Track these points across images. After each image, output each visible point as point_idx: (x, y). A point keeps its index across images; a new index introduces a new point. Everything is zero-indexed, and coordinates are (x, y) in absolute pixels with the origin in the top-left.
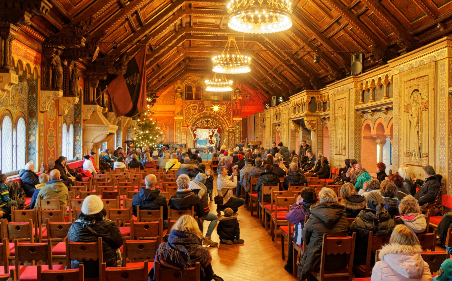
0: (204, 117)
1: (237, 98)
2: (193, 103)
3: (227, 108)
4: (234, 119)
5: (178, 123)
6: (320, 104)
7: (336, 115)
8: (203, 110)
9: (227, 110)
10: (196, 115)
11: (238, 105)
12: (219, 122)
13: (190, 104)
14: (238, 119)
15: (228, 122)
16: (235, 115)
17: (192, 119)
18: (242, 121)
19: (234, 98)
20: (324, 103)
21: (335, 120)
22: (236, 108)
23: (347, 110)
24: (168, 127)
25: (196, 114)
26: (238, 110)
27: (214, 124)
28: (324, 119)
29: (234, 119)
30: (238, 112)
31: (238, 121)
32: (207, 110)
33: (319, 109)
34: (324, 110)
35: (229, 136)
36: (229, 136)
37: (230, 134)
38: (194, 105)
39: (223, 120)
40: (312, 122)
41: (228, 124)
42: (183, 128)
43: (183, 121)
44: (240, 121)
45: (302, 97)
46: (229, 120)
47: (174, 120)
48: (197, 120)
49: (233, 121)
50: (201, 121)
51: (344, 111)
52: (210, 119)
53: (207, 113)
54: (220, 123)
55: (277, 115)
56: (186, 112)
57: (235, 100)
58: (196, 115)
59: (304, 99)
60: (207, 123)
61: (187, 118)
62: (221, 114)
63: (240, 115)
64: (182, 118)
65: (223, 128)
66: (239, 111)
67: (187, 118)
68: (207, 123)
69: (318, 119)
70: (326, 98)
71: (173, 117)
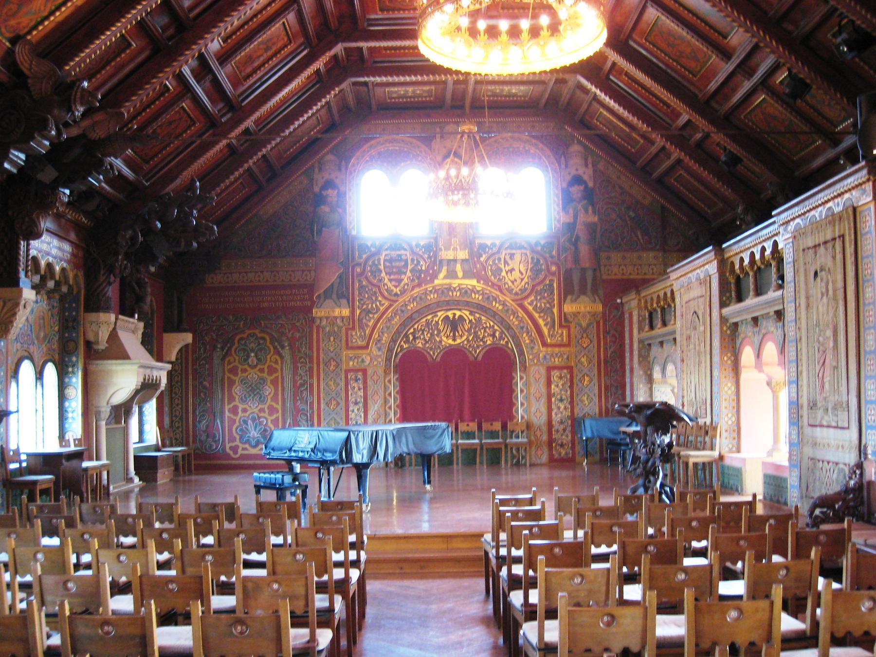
1: (576, 217)
4: (568, 308)
5: (330, 334)
8: (435, 276)
10: (406, 298)
12: (502, 322)
14: (583, 307)
15: (541, 322)
16: (568, 290)
18: (604, 314)
24: (286, 353)
25: (403, 292)
26: (583, 271)
27: (481, 334)
29: (568, 308)
30: (583, 280)
31: (584, 316)
32: (452, 274)
35: (549, 383)
36: (549, 383)
37: (555, 374)
39: (521, 313)
41: (545, 330)
42: (351, 353)
43: (352, 323)
44: (594, 315)
46: (546, 312)
47: (313, 319)
48: (411, 318)
49: (565, 321)
50: (428, 323)
52: (466, 314)
53: (449, 288)
54: (509, 328)
56: (361, 287)
58: (406, 298)
60: (454, 329)
61: (369, 312)
62: (510, 290)
63: (595, 291)
64: (346, 312)
65: (521, 353)
67: (369, 312)
68: (454, 329)
71: (309, 310)
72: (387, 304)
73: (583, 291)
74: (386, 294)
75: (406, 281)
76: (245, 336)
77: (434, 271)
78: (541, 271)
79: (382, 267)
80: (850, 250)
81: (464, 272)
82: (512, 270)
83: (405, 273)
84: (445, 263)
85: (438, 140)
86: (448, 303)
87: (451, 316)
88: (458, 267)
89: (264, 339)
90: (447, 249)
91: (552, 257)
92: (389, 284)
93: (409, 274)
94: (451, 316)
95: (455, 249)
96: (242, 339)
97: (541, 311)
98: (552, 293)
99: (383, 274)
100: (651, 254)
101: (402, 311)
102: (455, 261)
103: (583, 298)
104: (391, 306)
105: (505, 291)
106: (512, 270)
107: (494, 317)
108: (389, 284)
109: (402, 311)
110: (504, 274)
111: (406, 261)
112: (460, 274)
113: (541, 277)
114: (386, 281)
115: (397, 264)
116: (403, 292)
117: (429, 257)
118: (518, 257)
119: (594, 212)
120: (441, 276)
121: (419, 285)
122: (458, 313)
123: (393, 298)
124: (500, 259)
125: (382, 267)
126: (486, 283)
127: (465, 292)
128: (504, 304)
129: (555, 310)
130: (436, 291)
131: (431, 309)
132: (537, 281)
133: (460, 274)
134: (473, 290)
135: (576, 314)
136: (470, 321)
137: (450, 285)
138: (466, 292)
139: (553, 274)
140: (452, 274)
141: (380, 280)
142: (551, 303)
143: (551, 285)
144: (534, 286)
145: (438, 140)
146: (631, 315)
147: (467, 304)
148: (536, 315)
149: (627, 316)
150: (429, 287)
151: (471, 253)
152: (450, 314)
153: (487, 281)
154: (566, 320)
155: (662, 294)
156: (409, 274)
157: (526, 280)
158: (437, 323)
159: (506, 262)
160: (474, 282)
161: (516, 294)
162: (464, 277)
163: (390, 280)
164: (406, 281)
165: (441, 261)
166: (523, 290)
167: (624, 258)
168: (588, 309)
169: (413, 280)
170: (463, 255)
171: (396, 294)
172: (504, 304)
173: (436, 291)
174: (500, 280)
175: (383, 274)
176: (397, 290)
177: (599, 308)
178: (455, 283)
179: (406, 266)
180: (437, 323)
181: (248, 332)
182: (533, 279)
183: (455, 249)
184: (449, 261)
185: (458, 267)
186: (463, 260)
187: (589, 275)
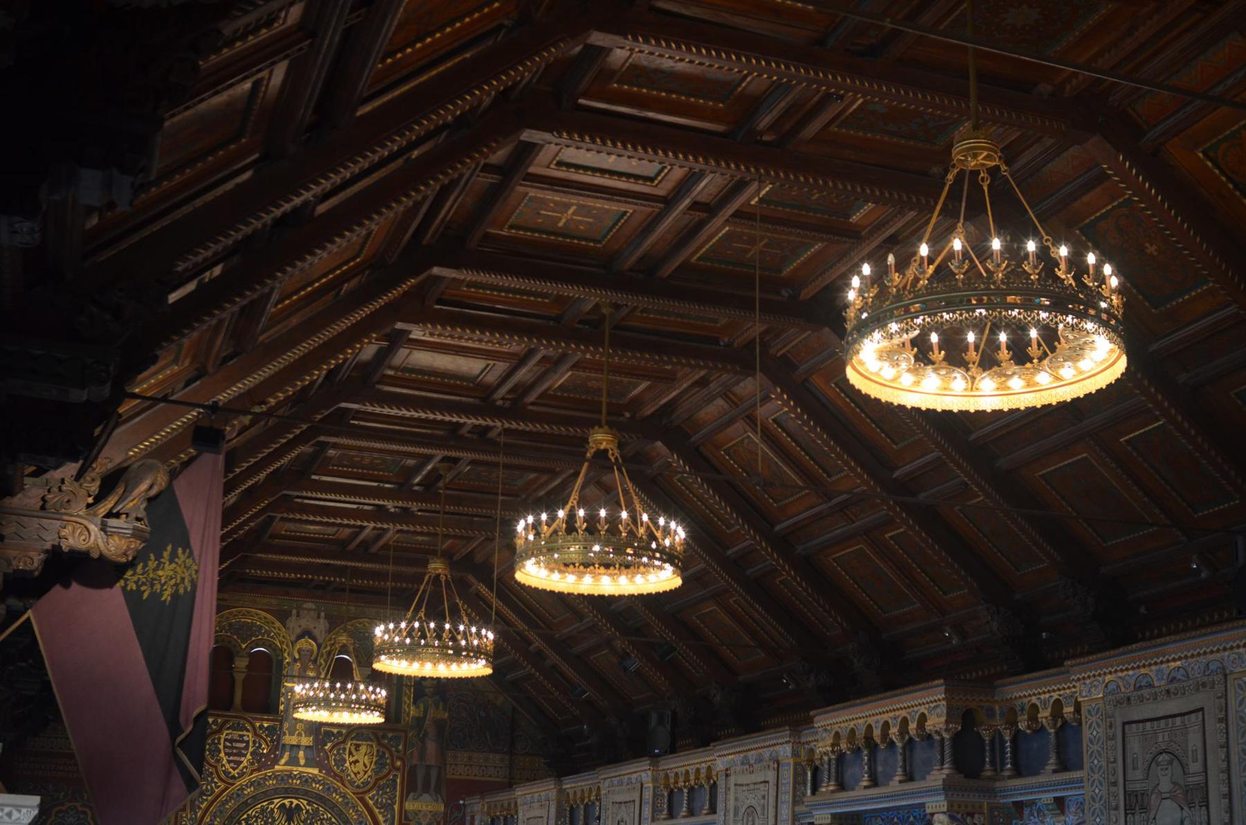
0: (276, 792)
1: (426, 712)
2: (232, 728)
3: (381, 756)
4: (409, 806)
6: (997, 738)
7: (1138, 787)
9: (380, 764)
10: (244, 781)
11: (431, 746)
13: (219, 731)
16: (411, 788)
17: (223, 797)
18: (445, 813)
19: (413, 711)
20: (1017, 736)
21: (1129, 809)
22: (422, 757)
23: (1216, 761)
25: (242, 774)
26: (429, 767)
28: (1019, 806)
29: (409, 806)
31: (425, 815)
33: (993, 763)
34: (1018, 772)
38: (236, 734)
39: (361, 808)
40: (969, 820)
44: (435, 814)
45: (928, 707)
46: (387, 808)
48: (246, 804)
50: (263, 810)
51: (1195, 767)
53: (290, 776)
55: (671, 793)
57: (419, 721)
58: (244, 781)
59: (923, 719)
62: (352, 782)
66: (434, 773)
69: (992, 808)
70: (1044, 714)
72: (223, 786)
73: (426, 789)
74: (223, 776)
75: (245, 763)
76: (64, 808)
77: (276, 756)
78: (383, 766)
79: (221, 747)
80: (637, 812)
81: (307, 759)
82: (356, 762)
83: (245, 756)
84: (288, 748)
85: (294, 618)
86: (286, 791)
87: (288, 805)
88: (301, 754)
89: (85, 813)
90: (292, 734)
91: (398, 751)
92: (227, 766)
93: (249, 756)
94: (288, 805)
95: (300, 734)
96: (60, 812)
97: (382, 806)
98: (395, 788)
99: (222, 755)
100: (498, 757)
101: (238, 795)
102: (298, 747)
103: (426, 796)
104: (227, 789)
105: (347, 783)
106: (356, 762)
107: (332, 808)
108: (227, 766)
109: (238, 795)
110: (347, 764)
111: (247, 742)
112: (302, 762)
113: (385, 771)
114: (225, 762)
115: (238, 745)
116: (242, 774)
117: (272, 741)
118: (363, 749)
119: (445, 709)
120: (283, 761)
121: (259, 770)
122: (295, 802)
123: (229, 779)
124: (344, 749)
125: (221, 747)
126: (328, 773)
127: (307, 780)
128: (344, 797)
129: (396, 807)
130: (276, 777)
131: (269, 795)
132: (381, 775)
133: (302, 762)
134: (314, 779)
135: (416, 813)
136: (307, 811)
137: (291, 771)
138: (306, 781)
139: (397, 769)
140: (294, 761)
141: (218, 761)
142: (392, 798)
143: (394, 781)
144: (377, 780)
145: (294, 618)
146: (473, 818)
147: (306, 793)
148: (377, 811)
149: (468, 818)
150: (269, 772)
151: (315, 740)
152: (286, 802)
153: (329, 771)
154: (407, 818)
155: (506, 805)
156: (249, 756)
157: (369, 773)
158: (272, 810)
159: (351, 753)
160: (316, 771)
161: (358, 787)
162: (305, 766)
163: (229, 762)
164: (245, 763)
165: (284, 745)
166: (366, 783)
167: (470, 758)
168: (430, 808)
169: (252, 764)
170: (306, 741)
171: (233, 777)
172: (344, 797)
173: (276, 777)
174: (343, 771)
175: (222, 755)
176: (235, 773)
177: (442, 809)
178: (296, 770)
179: (247, 748)
180: (272, 810)
181: (68, 805)
182: (376, 773)
183: (300, 734)
184: (293, 746)
185: (301, 754)
186: (307, 747)
187: (434, 773)
